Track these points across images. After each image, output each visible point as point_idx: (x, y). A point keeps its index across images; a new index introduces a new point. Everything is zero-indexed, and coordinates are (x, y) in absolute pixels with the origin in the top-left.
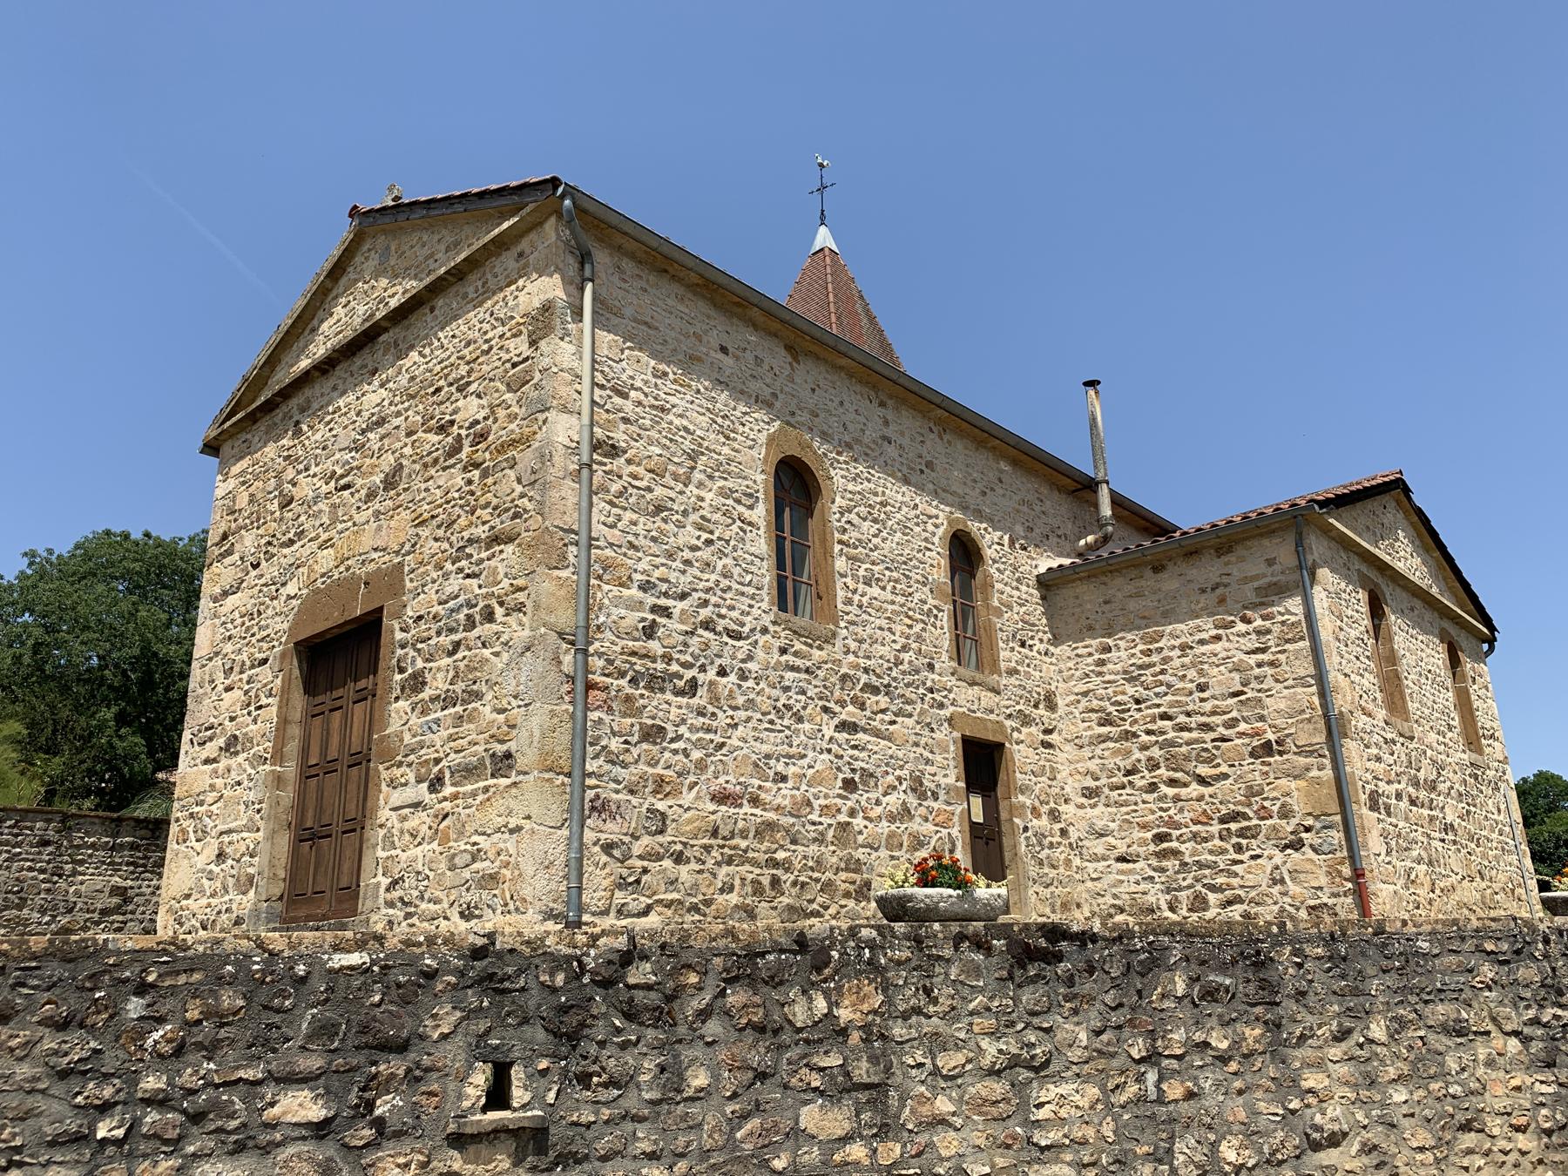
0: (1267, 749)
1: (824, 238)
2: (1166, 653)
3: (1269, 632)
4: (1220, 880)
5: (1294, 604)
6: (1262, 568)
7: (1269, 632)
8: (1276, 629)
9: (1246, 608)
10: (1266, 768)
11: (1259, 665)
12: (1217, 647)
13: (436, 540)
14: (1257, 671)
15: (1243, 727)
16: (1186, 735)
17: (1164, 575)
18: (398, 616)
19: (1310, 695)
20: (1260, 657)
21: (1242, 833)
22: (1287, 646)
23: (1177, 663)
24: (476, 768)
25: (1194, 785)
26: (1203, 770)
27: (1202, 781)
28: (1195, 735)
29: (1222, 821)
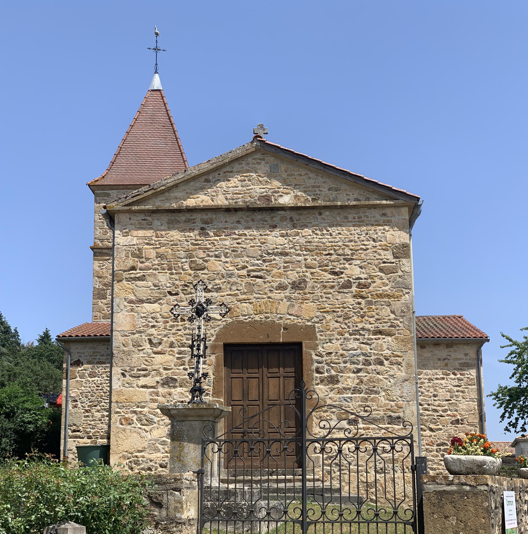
0: (457, 422)
1: (157, 83)
2: (422, 380)
3: (462, 380)
4: (435, 466)
5: (473, 372)
6: (462, 356)
7: (462, 380)
8: (465, 379)
9: (455, 370)
10: (456, 429)
11: (457, 391)
12: (443, 382)
13: (337, 322)
14: (456, 393)
15: (449, 412)
16: (427, 412)
17: (425, 350)
18: (315, 347)
19: (474, 405)
20: (458, 388)
21: (445, 450)
22: (468, 386)
23: (426, 385)
24: (379, 420)
25: (428, 431)
26: (432, 426)
27: (431, 430)
28: (430, 413)
29: (438, 445)
